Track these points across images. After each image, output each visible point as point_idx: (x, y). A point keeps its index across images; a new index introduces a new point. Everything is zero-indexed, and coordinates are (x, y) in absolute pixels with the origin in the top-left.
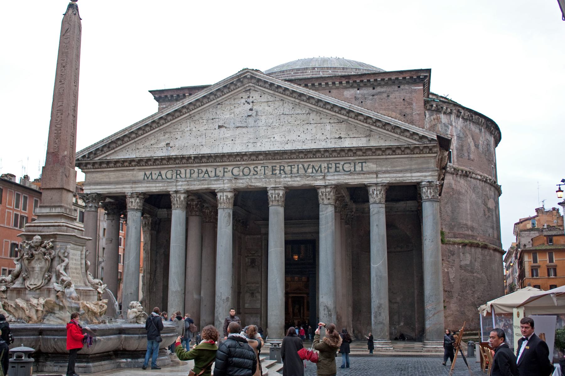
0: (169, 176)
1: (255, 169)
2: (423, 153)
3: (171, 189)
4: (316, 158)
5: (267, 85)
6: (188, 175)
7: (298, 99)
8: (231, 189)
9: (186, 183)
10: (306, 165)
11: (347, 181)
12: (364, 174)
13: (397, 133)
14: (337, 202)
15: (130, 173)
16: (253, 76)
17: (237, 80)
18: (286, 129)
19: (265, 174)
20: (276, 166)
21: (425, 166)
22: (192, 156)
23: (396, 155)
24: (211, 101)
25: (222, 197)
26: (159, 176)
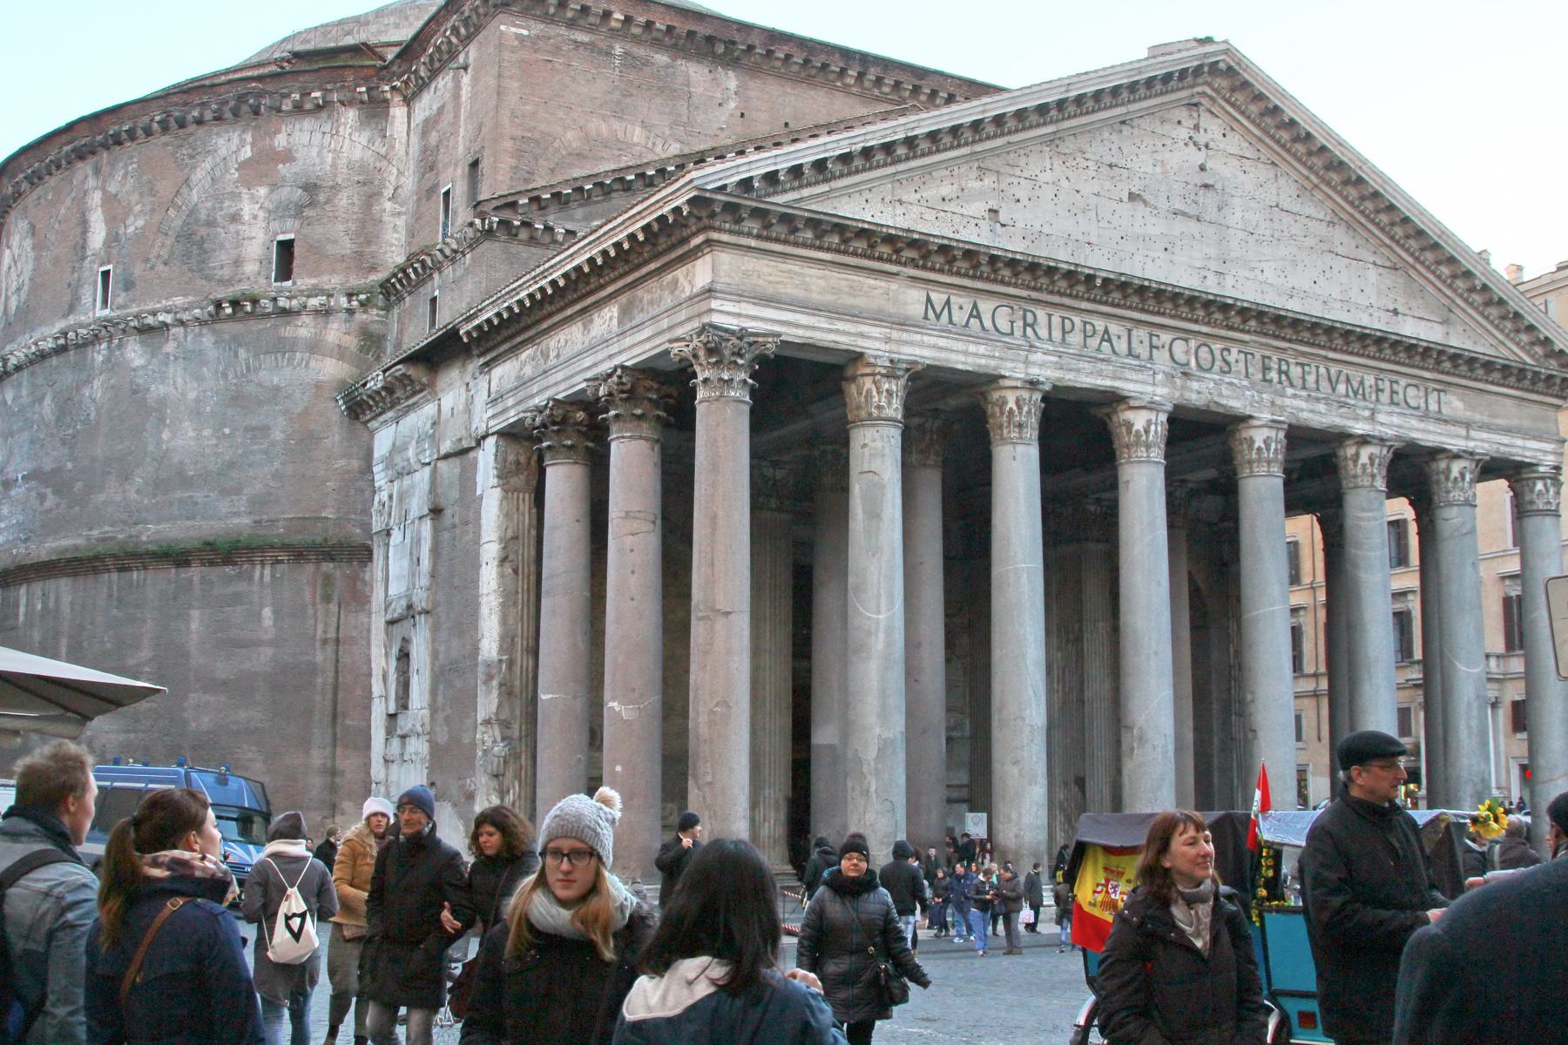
0: (1004, 325)
1: (1225, 353)
3: (1014, 370)
4: (1362, 356)
5: (1254, 109)
6: (1057, 334)
7: (1317, 174)
9: (1055, 359)
11: (1415, 435)
12: (1446, 421)
13: (1502, 331)
15: (877, 283)
16: (1237, 68)
19: (1247, 376)
20: (1270, 358)
21: (1542, 426)
23: (1503, 385)
24: (1117, 106)
25: (1153, 427)
26: (971, 316)
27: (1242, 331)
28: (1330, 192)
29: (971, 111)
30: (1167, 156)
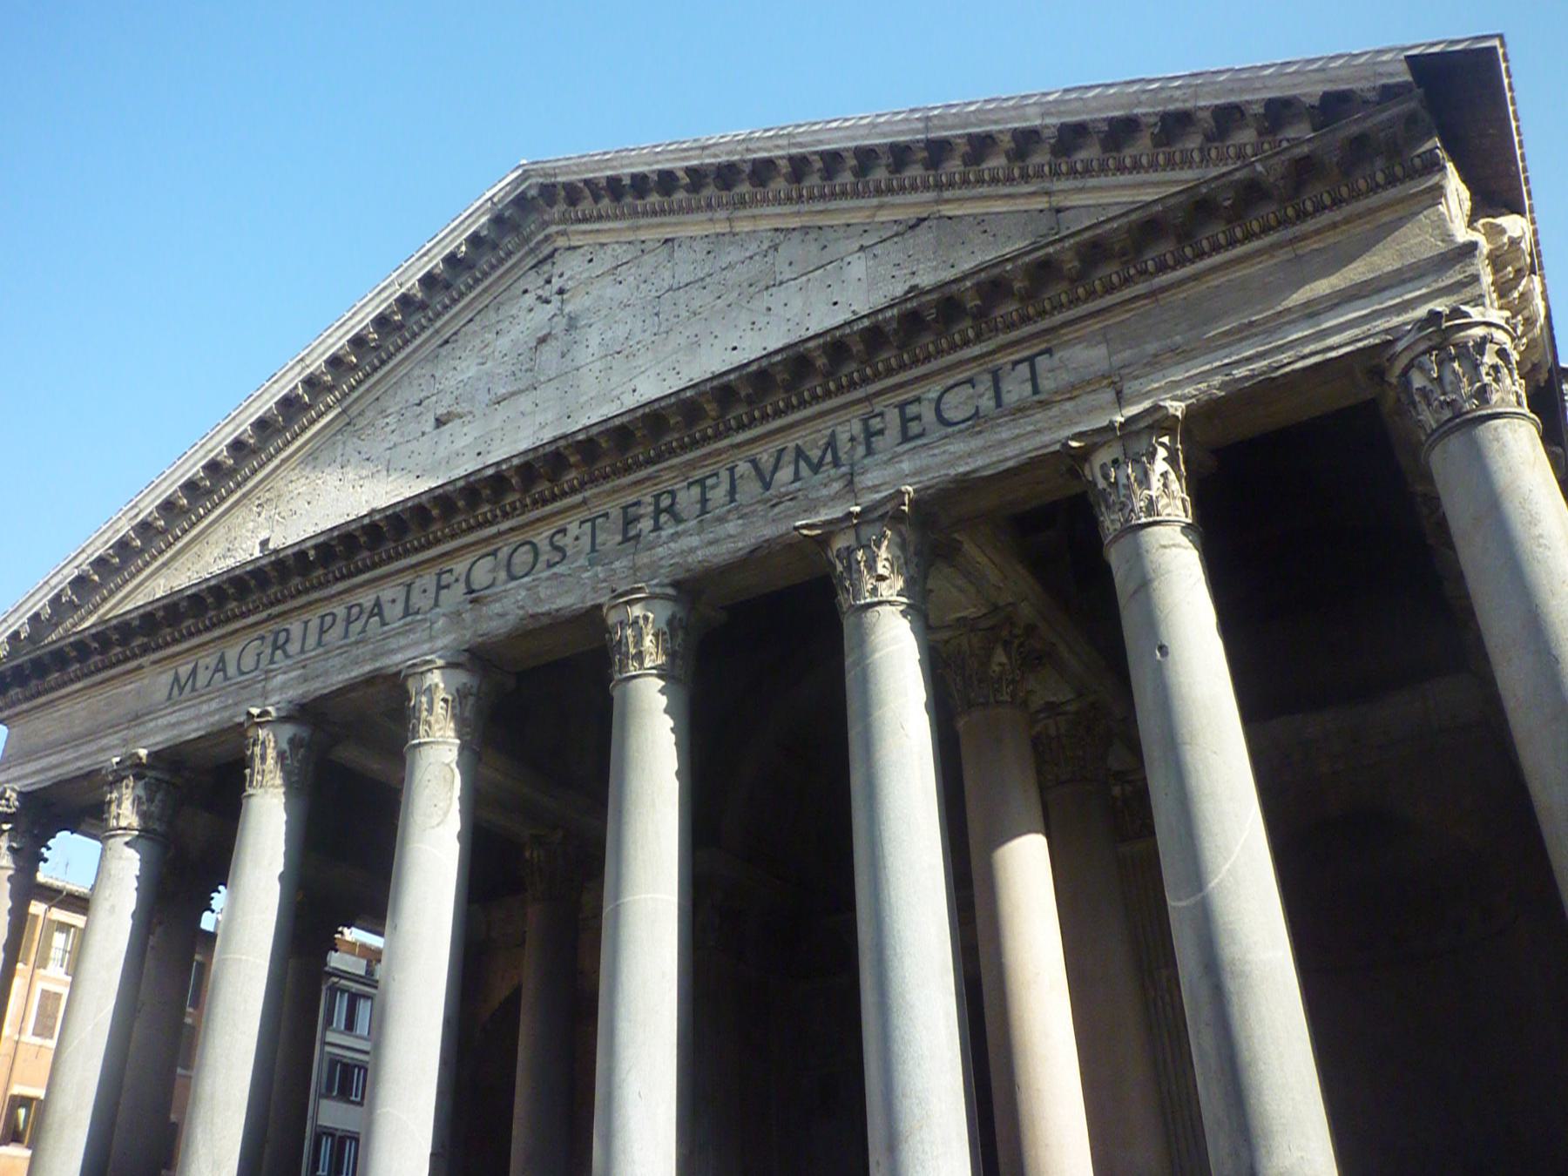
1: (557, 537)
2: (1356, 195)
4: (803, 404)
6: (312, 640)
8: (458, 651)
10: (766, 459)
11: (961, 470)
12: (1044, 404)
13: (1187, 162)
14: (1000, 657)
15: (132, 686)
17: (498, 221)
18: (683, 341)
19: (593, 550)
20: (637, 504)
22: (309, 544)
23: (1201, 255)
24: (415, 335)
26: (216, 670)
27: (564, 494)
28: (756, 211)
29: (191, 462)
30: (498, 343)
